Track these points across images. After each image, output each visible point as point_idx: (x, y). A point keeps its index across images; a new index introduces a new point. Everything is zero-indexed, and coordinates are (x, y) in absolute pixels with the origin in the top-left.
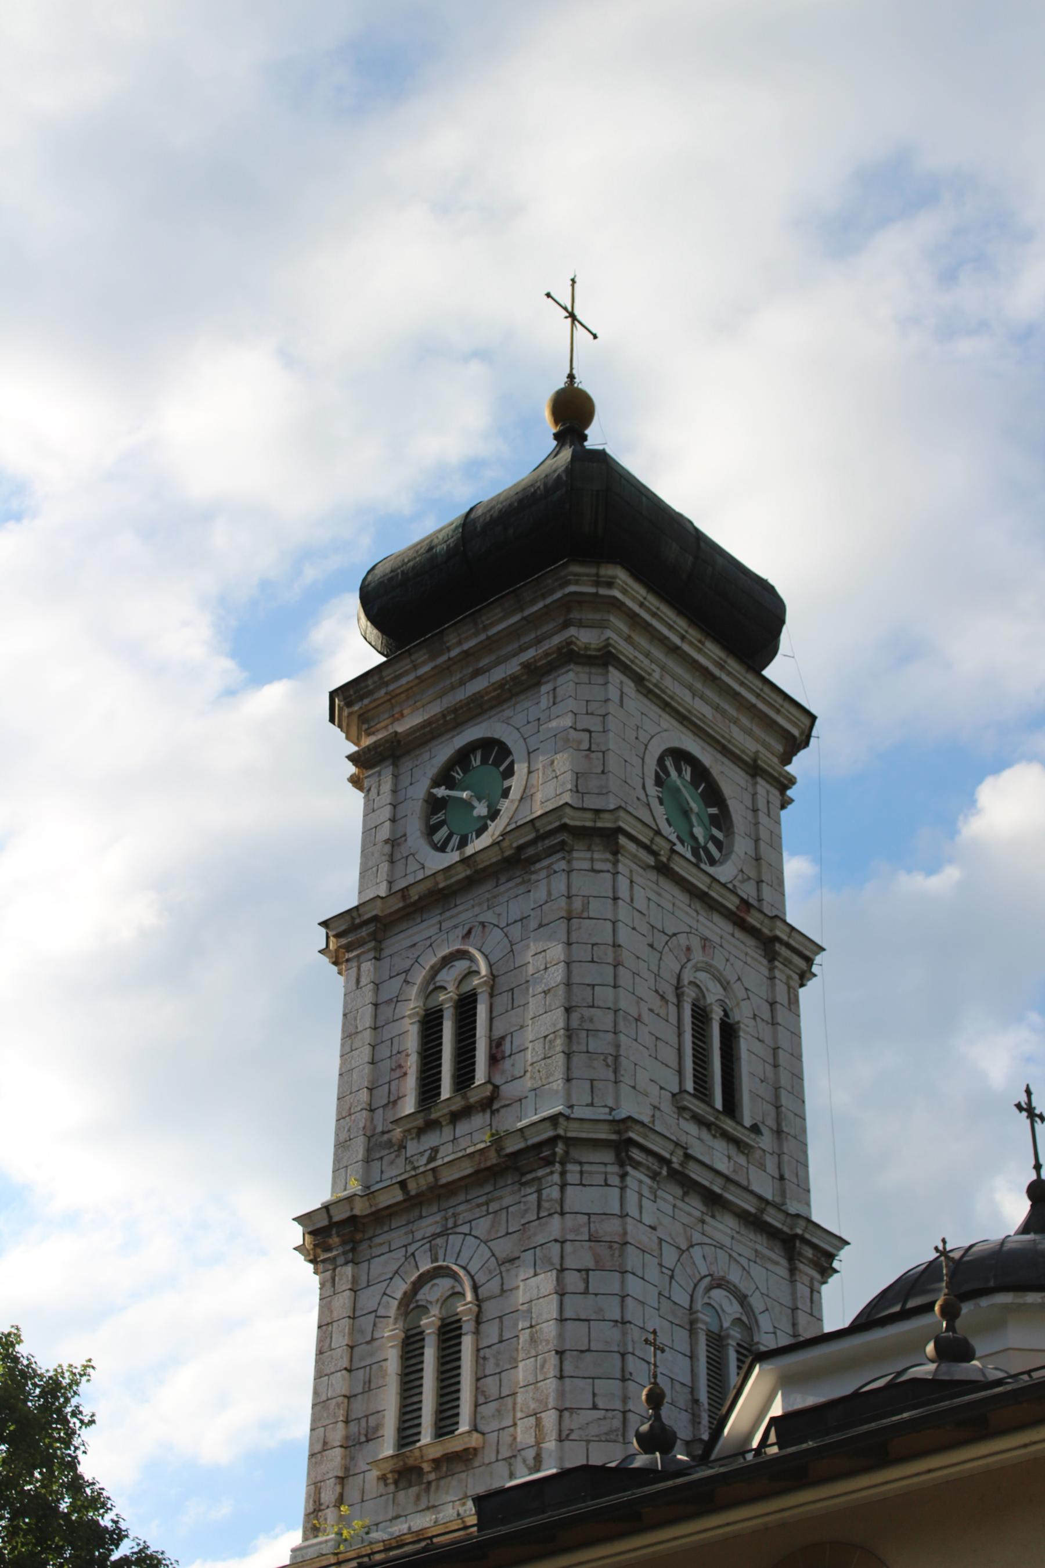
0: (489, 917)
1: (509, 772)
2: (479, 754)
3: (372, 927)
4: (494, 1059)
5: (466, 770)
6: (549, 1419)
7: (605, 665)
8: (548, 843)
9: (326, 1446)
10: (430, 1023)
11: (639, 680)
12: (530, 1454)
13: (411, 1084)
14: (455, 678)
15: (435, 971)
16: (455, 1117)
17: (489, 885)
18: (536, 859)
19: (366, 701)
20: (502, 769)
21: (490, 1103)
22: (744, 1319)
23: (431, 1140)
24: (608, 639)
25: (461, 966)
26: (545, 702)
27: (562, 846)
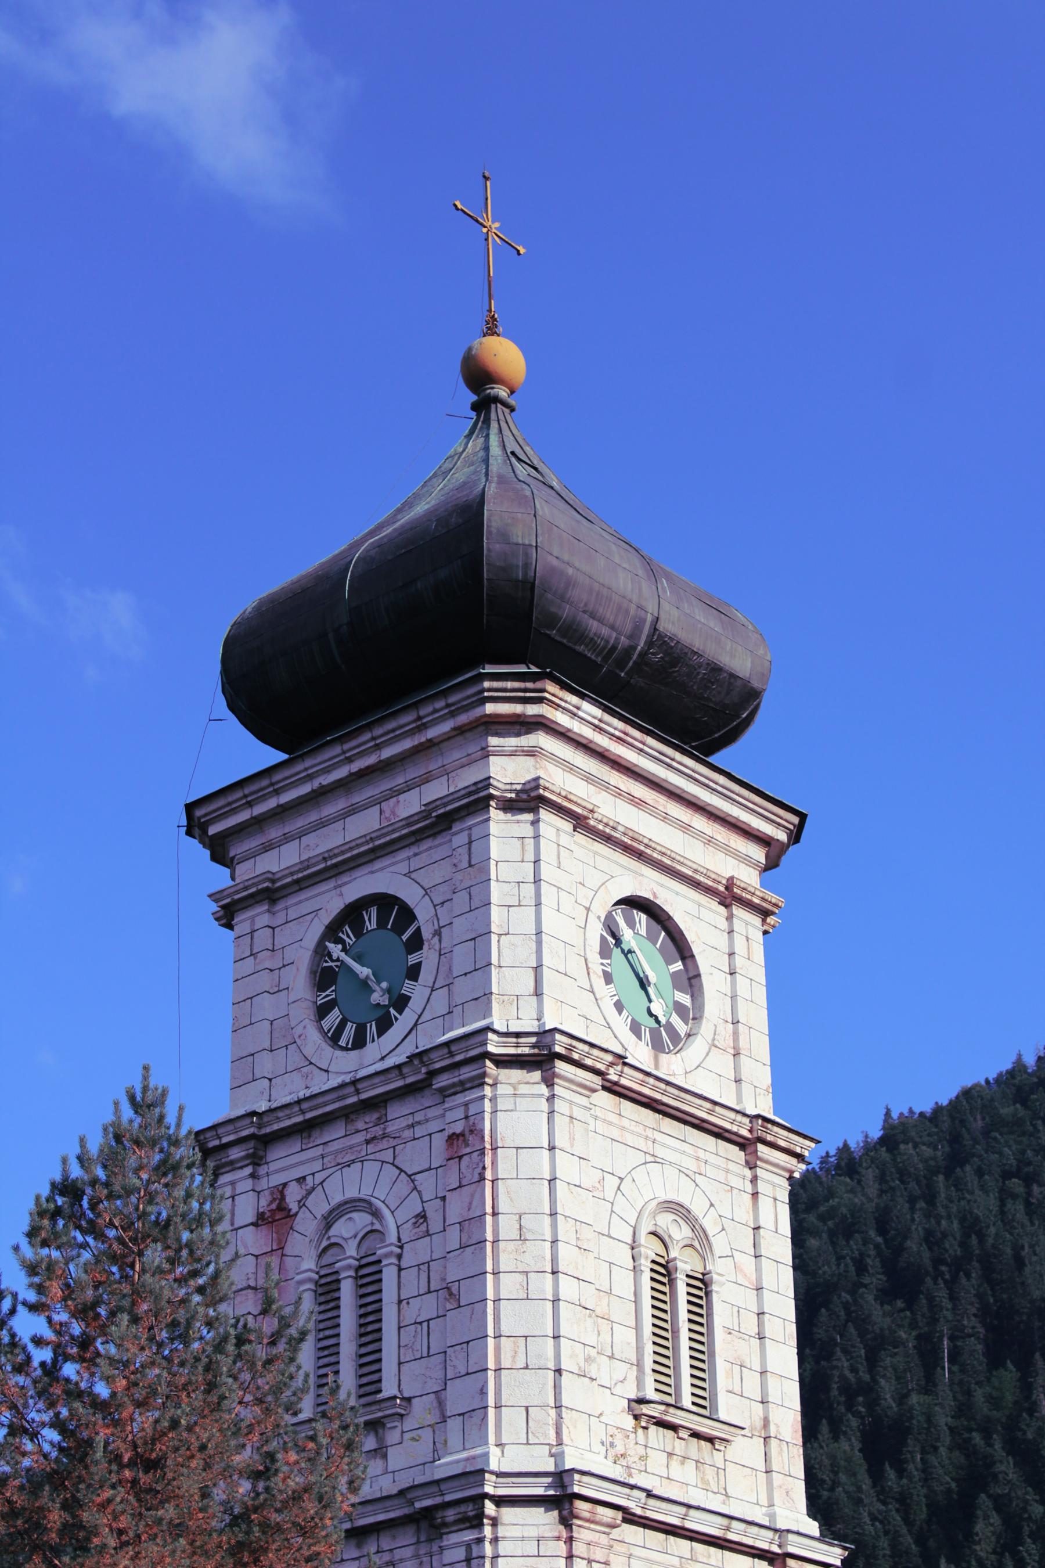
1: (416, 943)
2: (374, 911)
5: (359, 930)
7: (534, 810)
11: (580, 822)
15: (328, 1221)
20: (405, 937)
22: (696, 1244)
24: (538, 778)
25: (361, 1220)
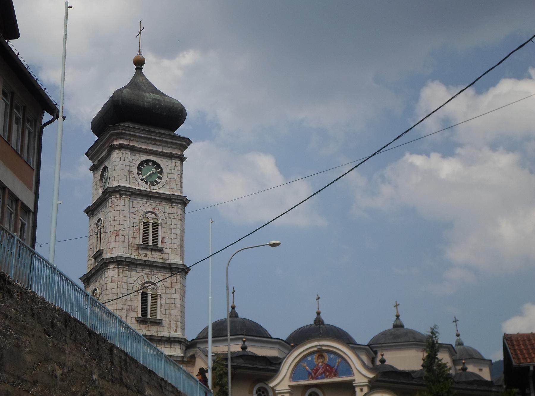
0: (160, 207)
3: (131, 194)
4: (161, 241)
6: (179, 323)
8: (178, 201)
9: (122, 308)
10: (146, 225)
12: (175, 329)
13: (141, 236)
14: (150, 142)
15: (146, 213)
16: (152, 250)
17: (160, 200)
18: (175, 203)
19: (127, 132)
21: (161, 251)
23: (146, 252)
26: (173, 164)
27: (180, 204)
